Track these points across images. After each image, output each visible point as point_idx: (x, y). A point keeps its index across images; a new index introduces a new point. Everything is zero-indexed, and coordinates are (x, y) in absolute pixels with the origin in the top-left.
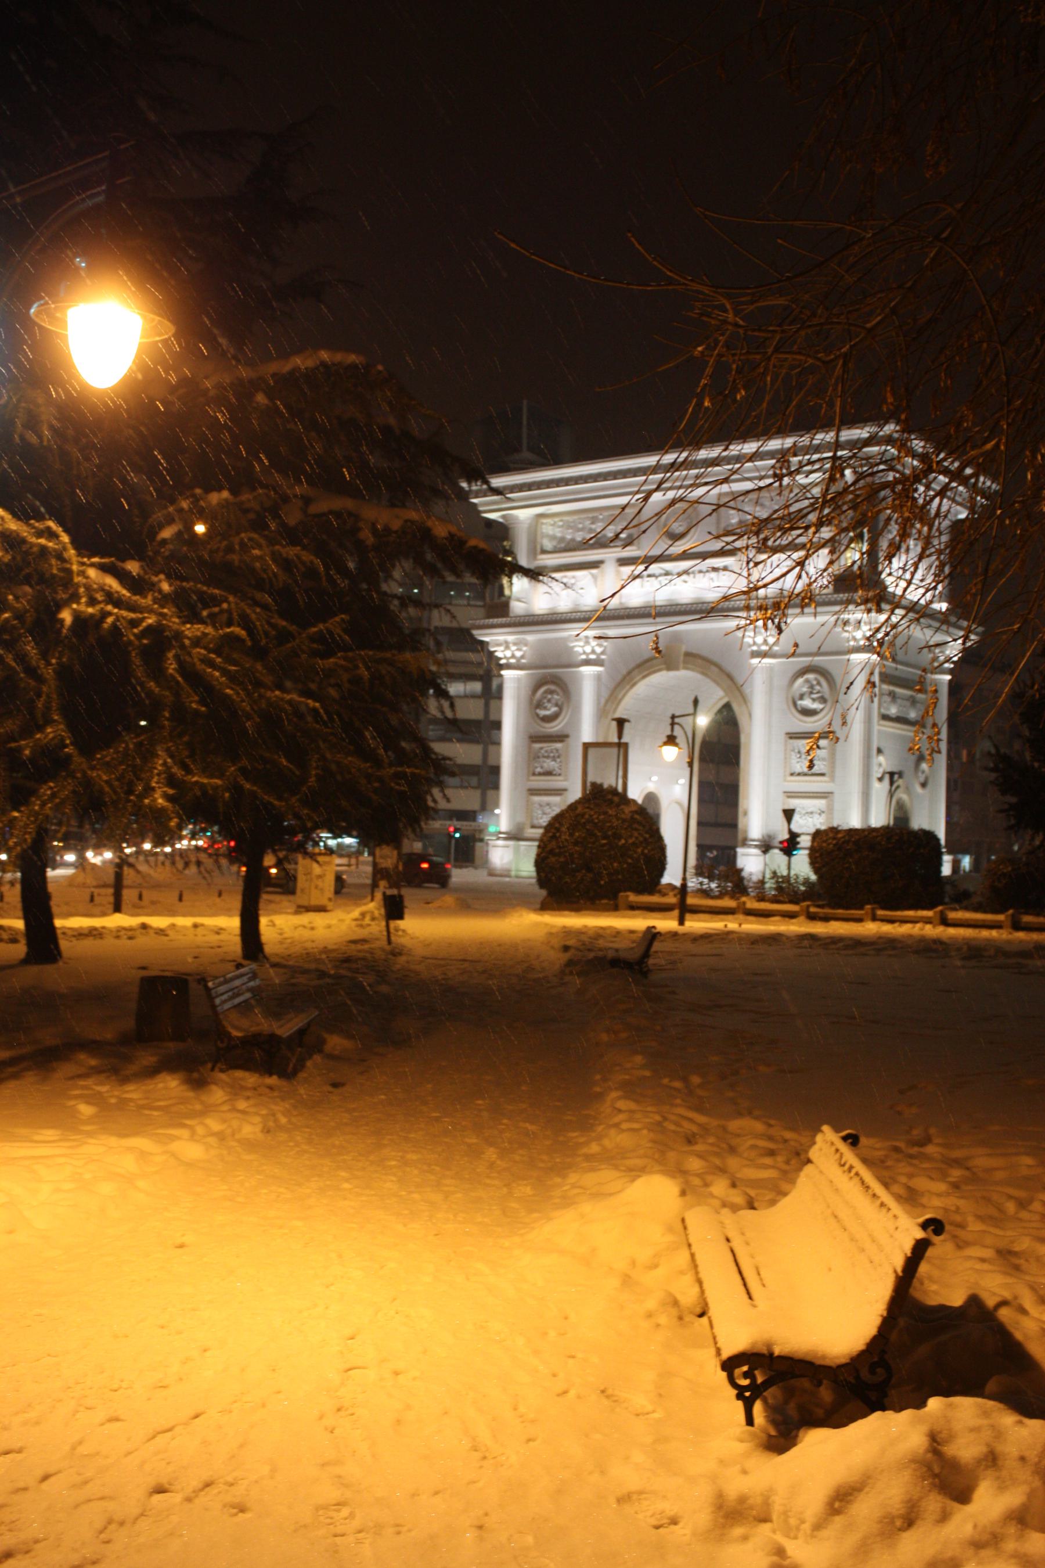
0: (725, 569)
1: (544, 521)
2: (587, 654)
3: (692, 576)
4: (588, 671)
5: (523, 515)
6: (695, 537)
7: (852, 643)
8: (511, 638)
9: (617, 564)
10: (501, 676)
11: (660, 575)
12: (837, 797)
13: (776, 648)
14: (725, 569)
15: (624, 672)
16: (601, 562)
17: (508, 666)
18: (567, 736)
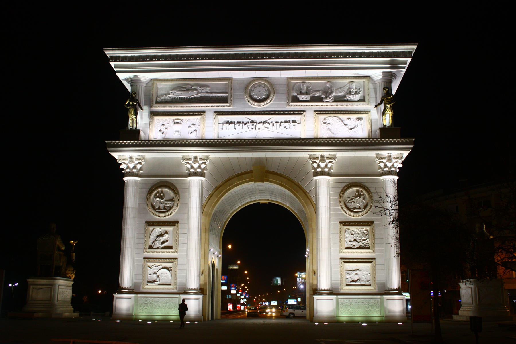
0: (294, 122)
1: (158, 83)
2: (195, 169)
3: (271, 124)
4: (195, 181)
5: (145, 77)
6: (272, 102)
7: (386, 169)
8: (136, 155)
9: (215, 114)
10: (124, 181)
11: (248, 123)
12: (377, 261)
13: (332, 171)
14: (294, 122)
15: (220, 182)
16: (204, 112)
17: (131, 174)
18: (177, 222)
